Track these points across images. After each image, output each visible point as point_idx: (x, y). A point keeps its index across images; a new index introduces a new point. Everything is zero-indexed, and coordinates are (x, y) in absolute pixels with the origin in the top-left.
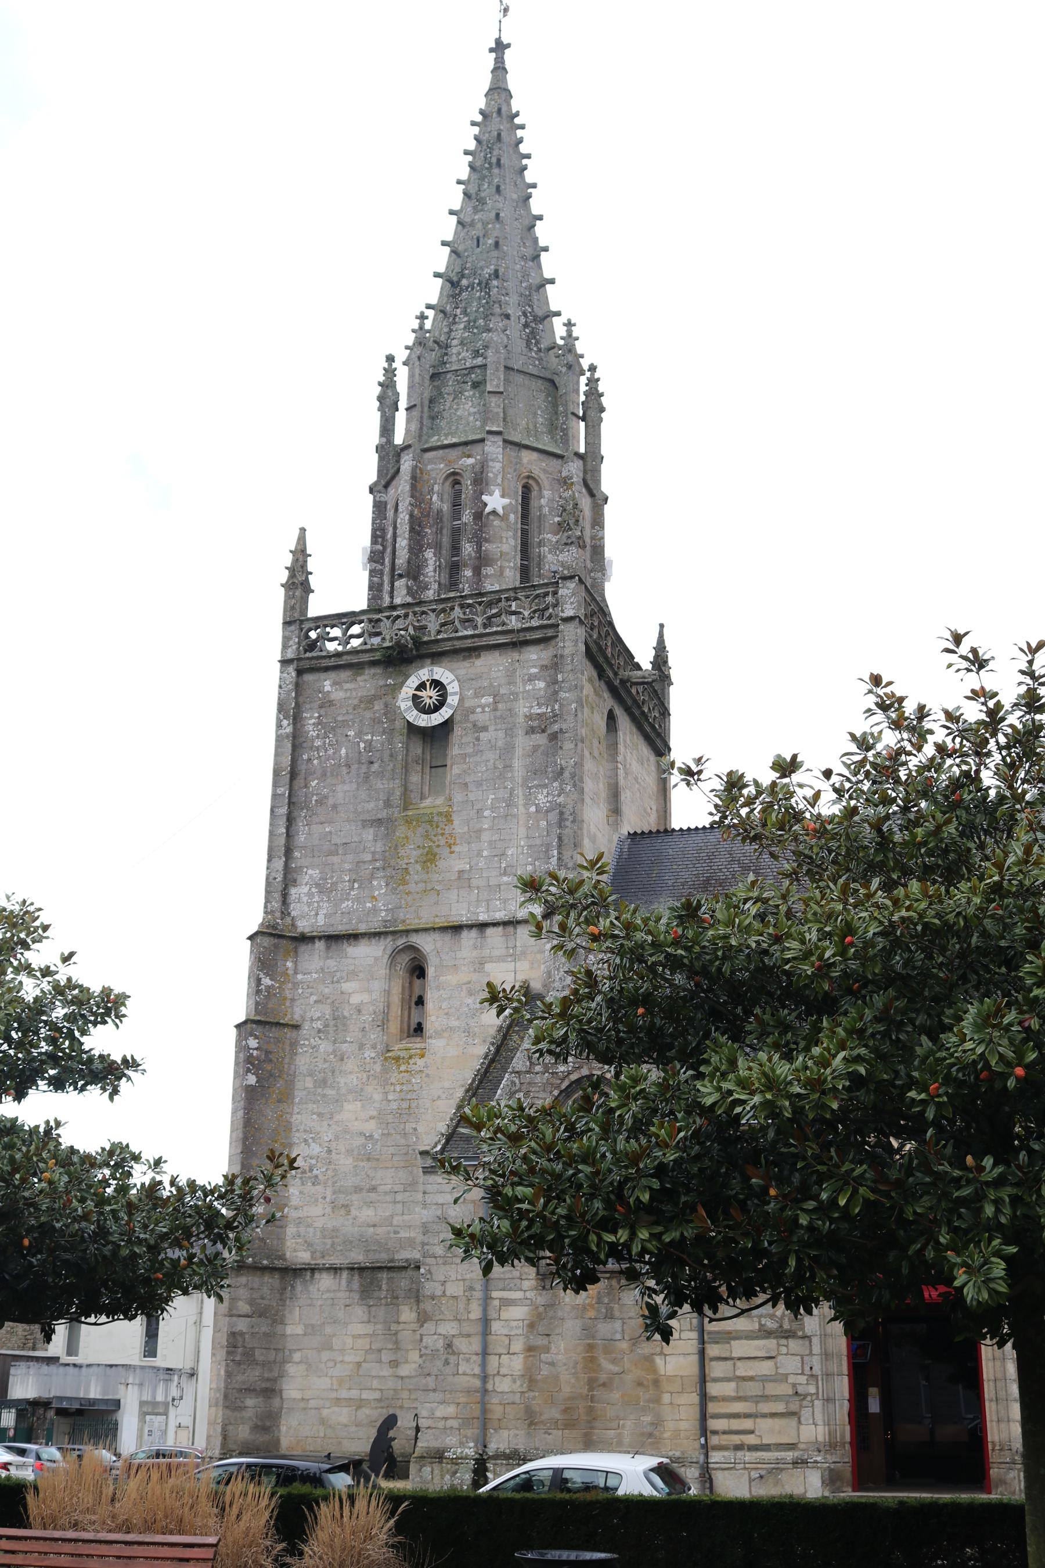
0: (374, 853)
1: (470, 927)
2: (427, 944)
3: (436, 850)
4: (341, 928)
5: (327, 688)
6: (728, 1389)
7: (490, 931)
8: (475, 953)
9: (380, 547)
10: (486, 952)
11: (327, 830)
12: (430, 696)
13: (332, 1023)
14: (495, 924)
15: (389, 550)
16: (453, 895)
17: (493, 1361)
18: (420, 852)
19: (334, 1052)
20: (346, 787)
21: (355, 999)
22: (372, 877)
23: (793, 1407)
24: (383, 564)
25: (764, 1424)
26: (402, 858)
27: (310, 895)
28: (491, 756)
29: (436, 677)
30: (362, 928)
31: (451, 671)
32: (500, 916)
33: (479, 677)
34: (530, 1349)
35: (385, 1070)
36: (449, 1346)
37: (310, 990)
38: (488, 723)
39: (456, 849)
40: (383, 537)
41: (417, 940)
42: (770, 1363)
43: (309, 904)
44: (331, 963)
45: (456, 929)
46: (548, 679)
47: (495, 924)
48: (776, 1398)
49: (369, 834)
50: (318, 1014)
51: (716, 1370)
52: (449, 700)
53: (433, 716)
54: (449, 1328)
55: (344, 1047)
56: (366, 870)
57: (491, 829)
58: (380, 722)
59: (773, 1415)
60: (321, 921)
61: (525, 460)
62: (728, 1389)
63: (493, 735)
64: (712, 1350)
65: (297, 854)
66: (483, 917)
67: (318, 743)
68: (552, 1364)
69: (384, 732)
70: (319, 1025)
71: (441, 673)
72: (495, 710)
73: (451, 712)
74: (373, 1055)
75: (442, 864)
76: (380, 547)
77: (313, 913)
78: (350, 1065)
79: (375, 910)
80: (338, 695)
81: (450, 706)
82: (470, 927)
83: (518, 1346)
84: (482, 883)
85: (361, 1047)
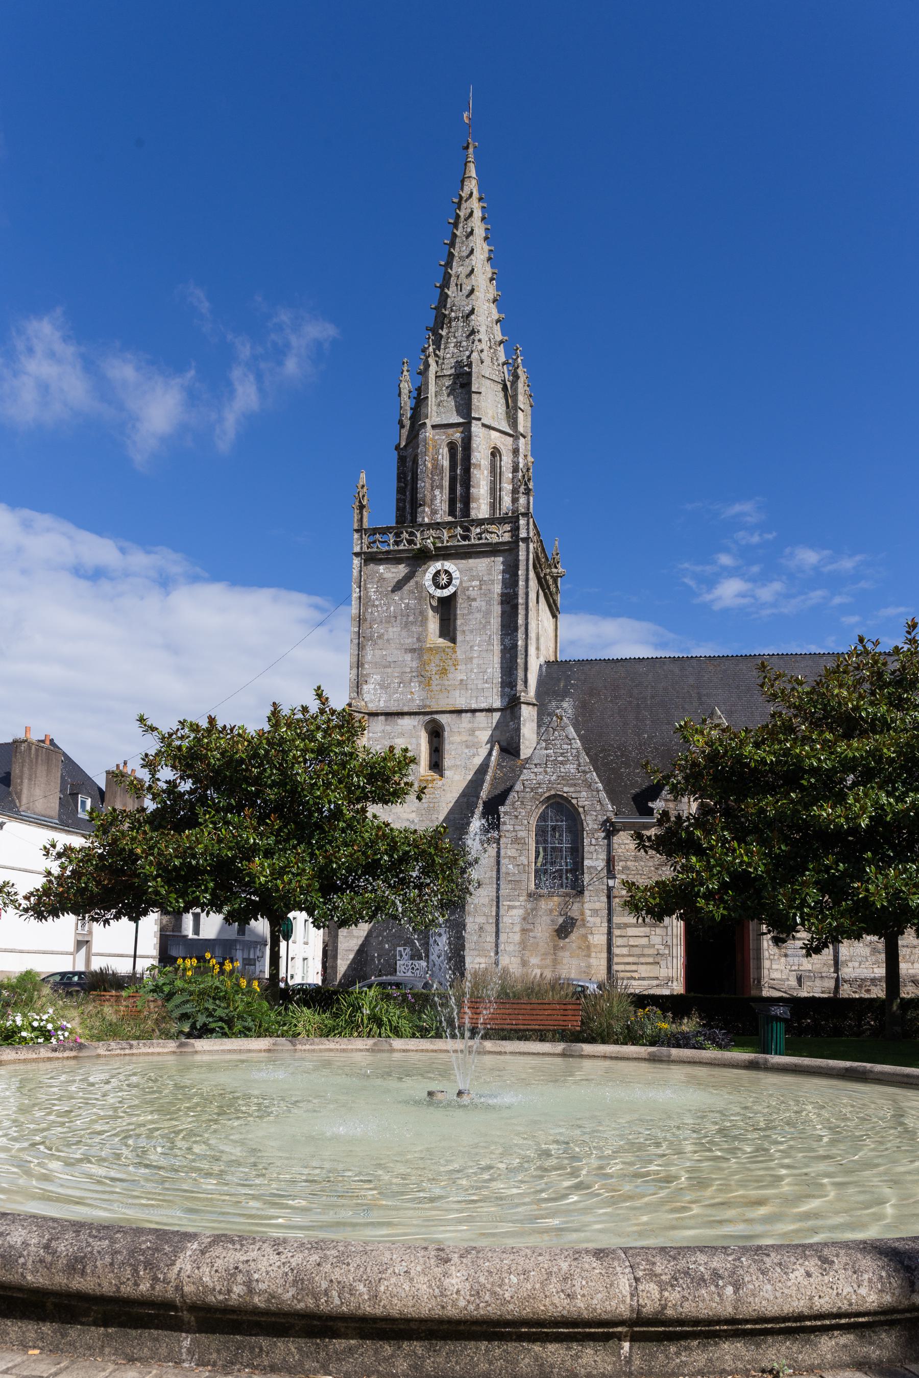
1: (466, 711)
2: (444, 719)
4: (394, 709)
5: (382, 571)
6: (625, 951)
7: (477, 714)
8: (470, 725)
9: (402, 485)
10: (476, 725)
12: (444, 579)
14: (481, 711)
15: (409, 487)
16: (457, 693)
17: (503, 937)
20: (395, 629)
22: (411, 681)
23: (657, 960)
24: (405, 495)
25: (642, 968)
26: (427, 671)
27: (375, 689)
28: (479, 616)
29: (446, 568)
30: (406, 709)
31: (455, 565)
32: (483, 705)
33: (471, 569)
34: (524, 931)
36: (481, 928)
39: (459, 667)
40: (405, 478)
42: (647, 939)
43: (374, 695)
44: (388, 728)
45: (459, 712)
47: (481, 711)
48: (649, 955)
49: (408, 657)
51: (617, 941)
52: (454, 582)
53: (445, 591)
54: (481, 920)
57: (478, 657)
59: (647, 964)
60: (382, 704)
61: (493, 437)
62: (625, 951)
63: (478, 604)
64: (616, 932)
65: (366, 666)
66: (474, 706)
67: (377, 603)
68: (535, 938)
69: (416, 599)
71: (449, 565)
72: (481, 589)
73: (454, 589)
75: (450, 676)
76: (402, 485)
79: (412, 700)
80: (388, 575)
81: (455, 586)
82: (466, 711)
83: (517, 928)
84: (473, 687)
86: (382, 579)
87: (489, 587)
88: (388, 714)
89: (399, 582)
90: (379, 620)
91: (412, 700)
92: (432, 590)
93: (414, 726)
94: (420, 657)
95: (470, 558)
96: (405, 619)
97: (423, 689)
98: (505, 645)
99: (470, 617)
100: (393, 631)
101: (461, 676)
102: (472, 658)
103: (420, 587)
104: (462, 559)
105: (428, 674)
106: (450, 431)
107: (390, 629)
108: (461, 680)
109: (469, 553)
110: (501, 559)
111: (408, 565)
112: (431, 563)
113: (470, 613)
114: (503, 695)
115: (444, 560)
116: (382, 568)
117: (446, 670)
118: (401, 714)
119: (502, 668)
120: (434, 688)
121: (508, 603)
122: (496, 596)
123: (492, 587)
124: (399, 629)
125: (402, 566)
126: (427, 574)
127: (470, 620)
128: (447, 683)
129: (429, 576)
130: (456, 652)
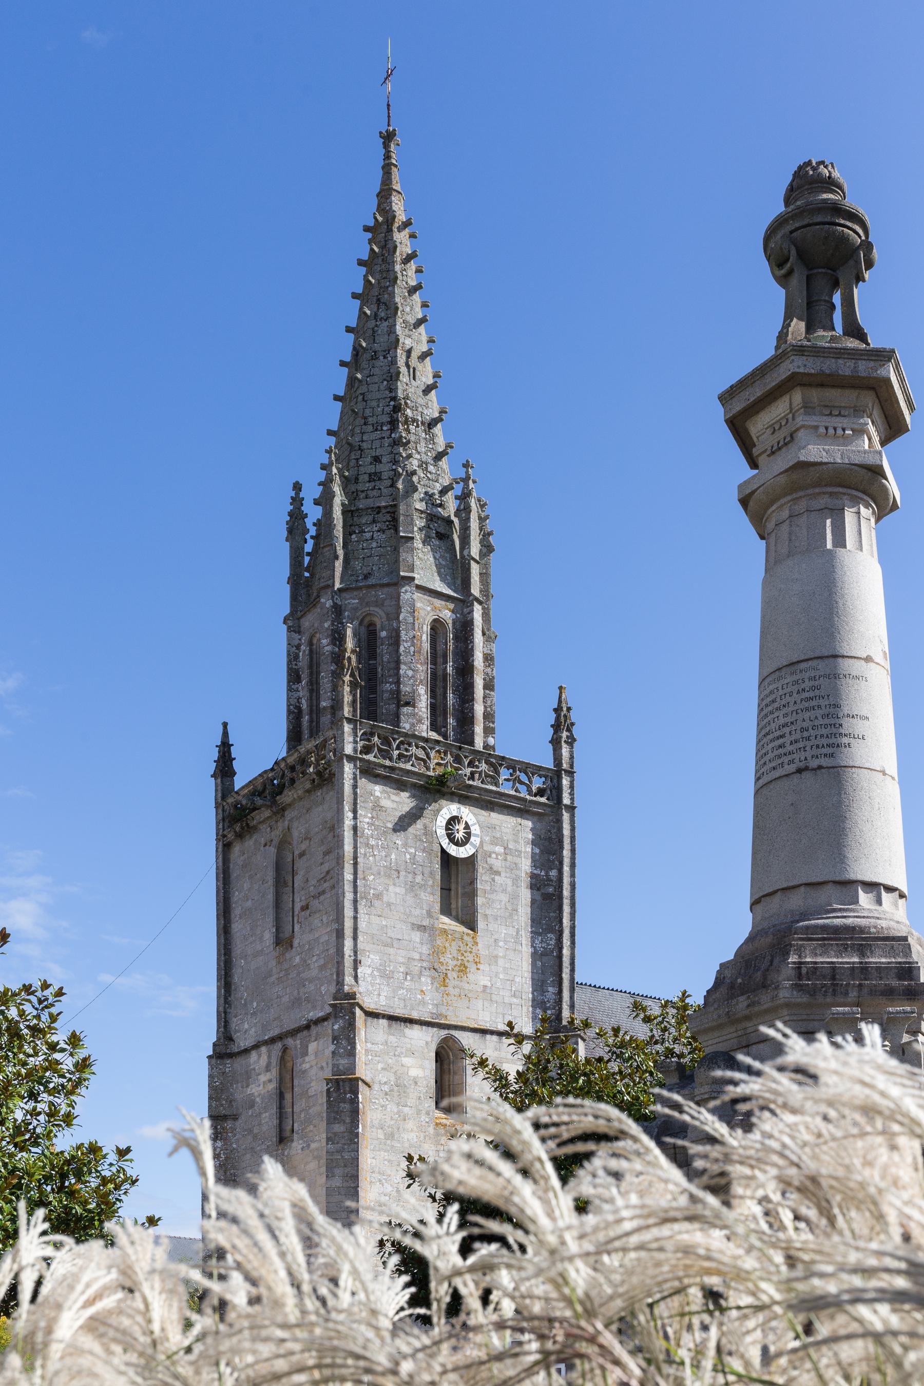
0: (421, 953)
1: (492, 1033)
3: (466, 964)
4: (399, 1012)
5: (378, 794)
11: (384, 923)
13: (396, 1088)
16: (480, 1003)
18: (455, 962)
19: (399, 1112)
20: (398, 890)
21: (414, 1072)
22: (420, 974)
26: (442, 963)
27: (372, 975)
28: (504, 898)
30: (415, 1015)
31: (474, 814)
35: (437, 1135)
37: (377, 1058)
38: (500, 869)
39: (481, 966)
41: (457, 1034)
43: (372, 985)
44: (392, 1039)
45: (484, 1032)
46: (542, 847)
49: (416, 936)
50: (385, 1080)
52: (472, 839)
53: (462, 849)
55: (406, 1110)
56: (416, 967)
57: (504, 957)
58: (421, 840)
60: (383, 1001)
67: (372, 842)
69: (424, 851)
70: (386, 1088)
71: (467, 814)
74: (427, 1120)
77: (376, 993)
78: (410, 1125)
79: (423, 1003)
80: (386, 803)
85: (419, 1112)
86: (377, 807)
87: (517, 860)
88: (392, 1018)
89: (401, 818)
90: (375, 870)
91: (423, 1003)
92: (445, 842)
93: (427, 1043)
94: (432, 938)
95: (492, 810)
96: (410, 876)
97: (437, 990)
98: (535, 948)
99: (493, 896)
100: (395, 892)
101: (484, 981)
102: (496, 957)
103: (429, 833)
104: (482, 808)
105: (443, 968)
106: (438, 603)
107: (391, 888)
108: (485, 987)
109: (491, 803)
110: (529, 824)
111: (413, 796)
112: (443, 802)
113: (493, 891)
114: (534, 1018)
115: (459, 803)
116: (378, 789)
117: (466, 967)
118: (410, 1021)
119: (533, 979)
120: (450, 989)
121: (538, 889)
122: (523, 875)
123: (517, 860)
124: (403, 891)
125: (405, 795)
126: (439, 819)
127: (493, 901)
128: (466, 986)
129: (441, 821)
130: (476, 944)
